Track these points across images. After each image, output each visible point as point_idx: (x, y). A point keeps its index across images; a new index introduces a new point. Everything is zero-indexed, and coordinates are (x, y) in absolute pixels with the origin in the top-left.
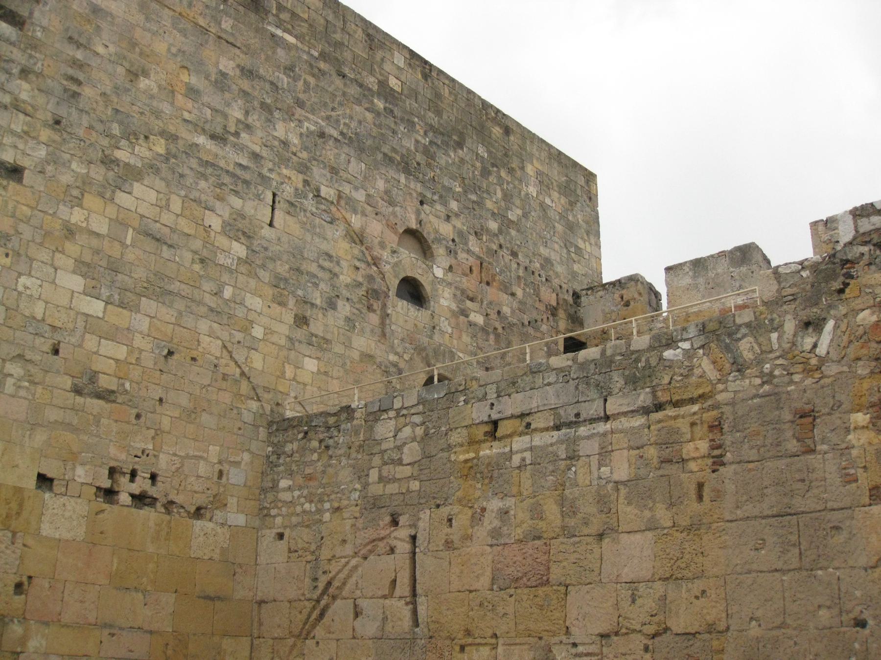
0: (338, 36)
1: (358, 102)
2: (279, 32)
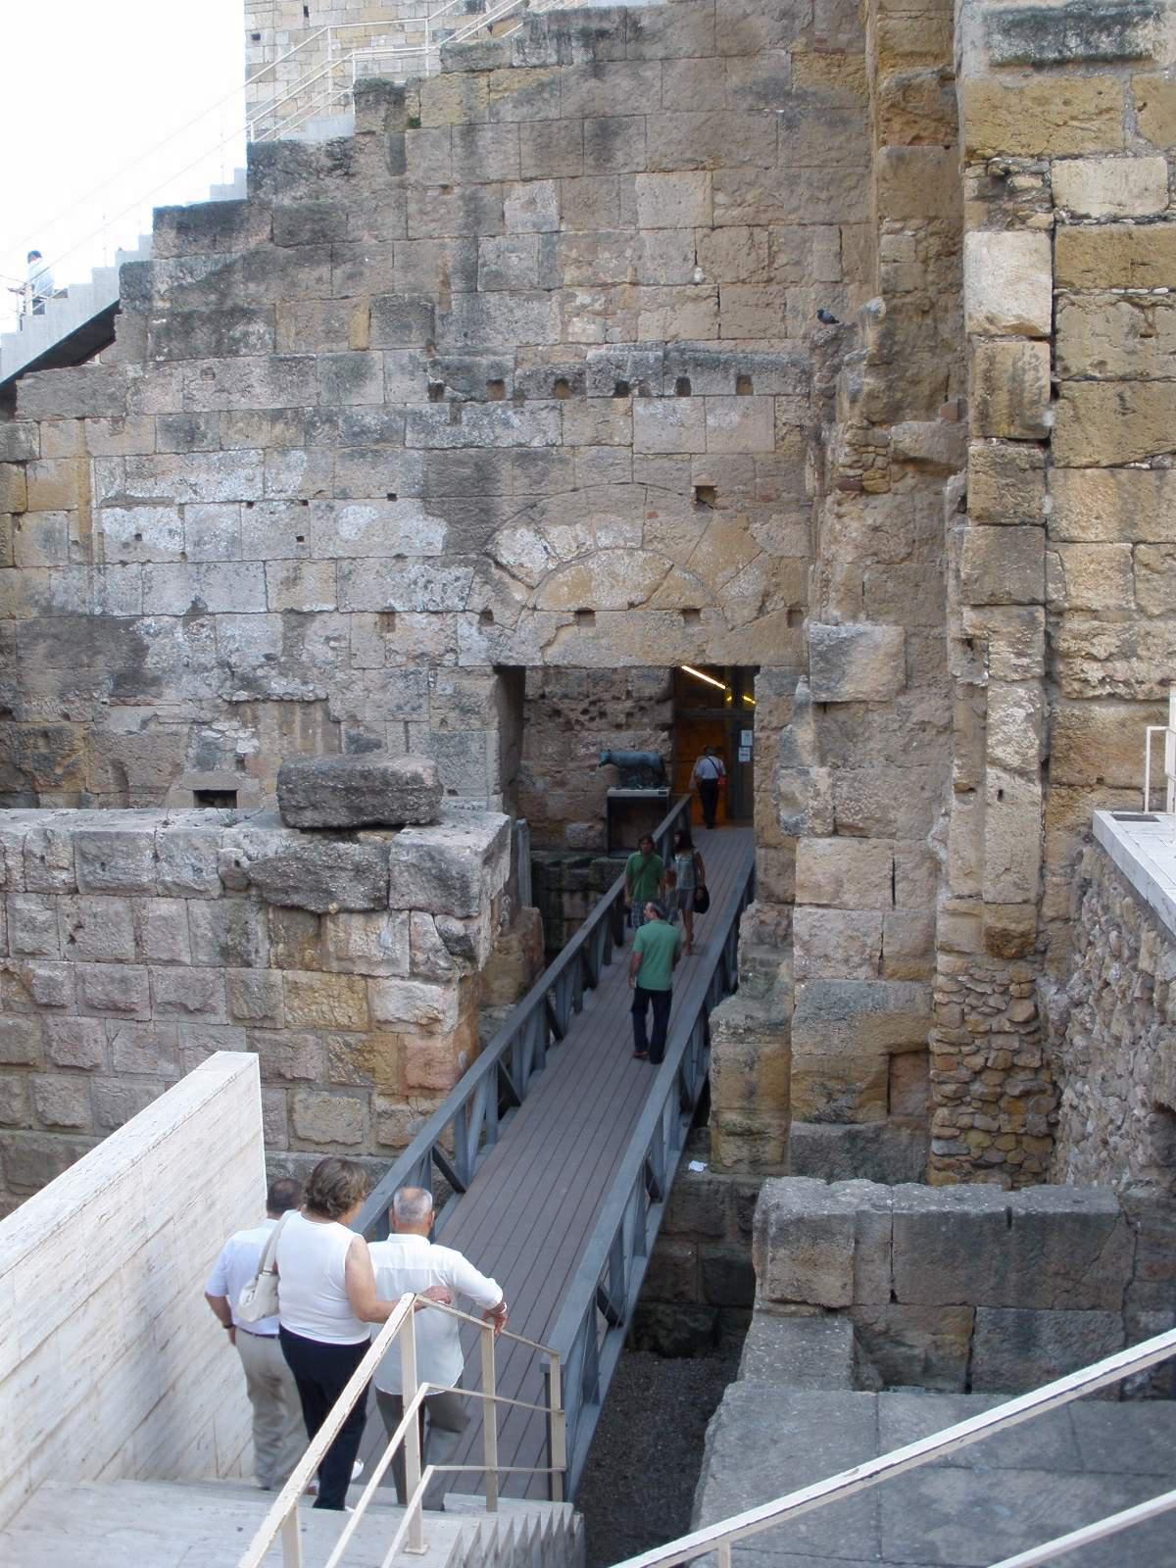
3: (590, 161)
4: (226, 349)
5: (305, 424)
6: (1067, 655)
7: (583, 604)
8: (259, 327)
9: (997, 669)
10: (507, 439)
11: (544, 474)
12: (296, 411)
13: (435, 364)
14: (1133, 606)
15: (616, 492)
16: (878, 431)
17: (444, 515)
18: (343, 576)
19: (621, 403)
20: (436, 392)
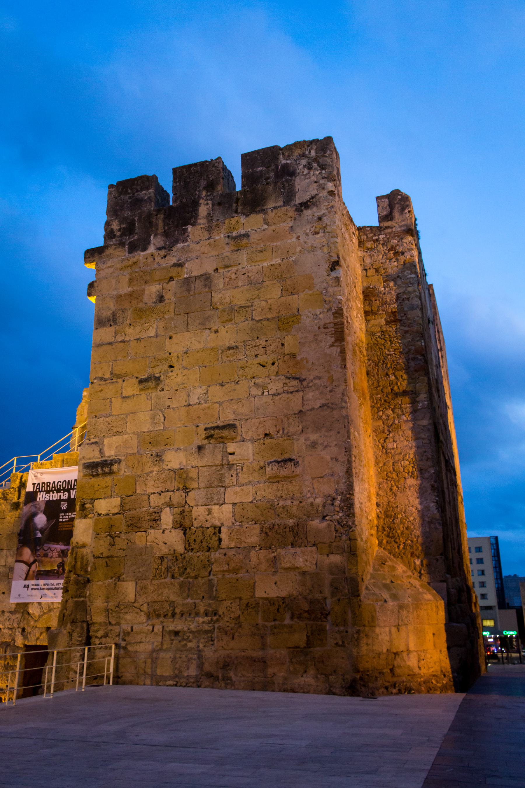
14: (108, 622)
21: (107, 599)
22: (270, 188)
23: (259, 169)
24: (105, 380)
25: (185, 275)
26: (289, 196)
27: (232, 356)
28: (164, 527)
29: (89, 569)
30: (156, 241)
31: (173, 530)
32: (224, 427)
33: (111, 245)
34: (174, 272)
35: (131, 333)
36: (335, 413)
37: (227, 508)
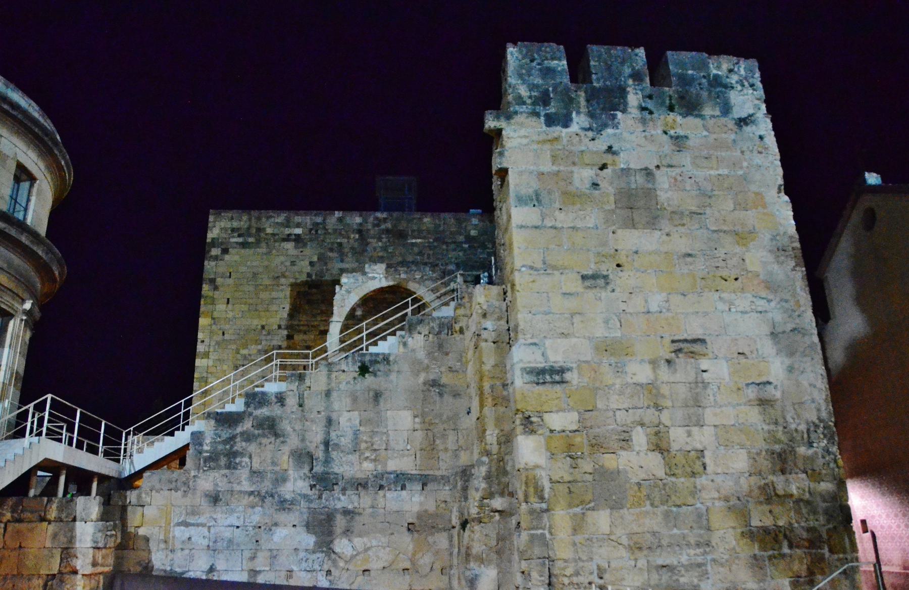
0: (442, 228)
1: (455, 250)
2: (414, 241)
3: (371, 406)
4: (231, 466)
5: (262, 497)
6: (556, 576)
7: (365, 568)
8: (246, 459)
9: (534, 581)
10: (339, 505)
11: (352, 518)
12: (259, 492)
13: (313, 477)
15: (380, 526)
16: (485, 501)
17: (315, 533)
18: (273, 557)
19: (381, 493)
20: (312, 487)
21: (575, 531)
22: (705, 94)
23: (690, 72)
24: (537, 270)
25: (622, 166)
26: (726, 109)
27: (691, 264)
28: (637, 448)
29: (546, 496)
30: (579, 120)
31: (649, 453)
32: (695, 341)
33: (521, 113)
34: (608, 159)
35: (563, 219)
36: (806, 338)
37: (708, 431)
